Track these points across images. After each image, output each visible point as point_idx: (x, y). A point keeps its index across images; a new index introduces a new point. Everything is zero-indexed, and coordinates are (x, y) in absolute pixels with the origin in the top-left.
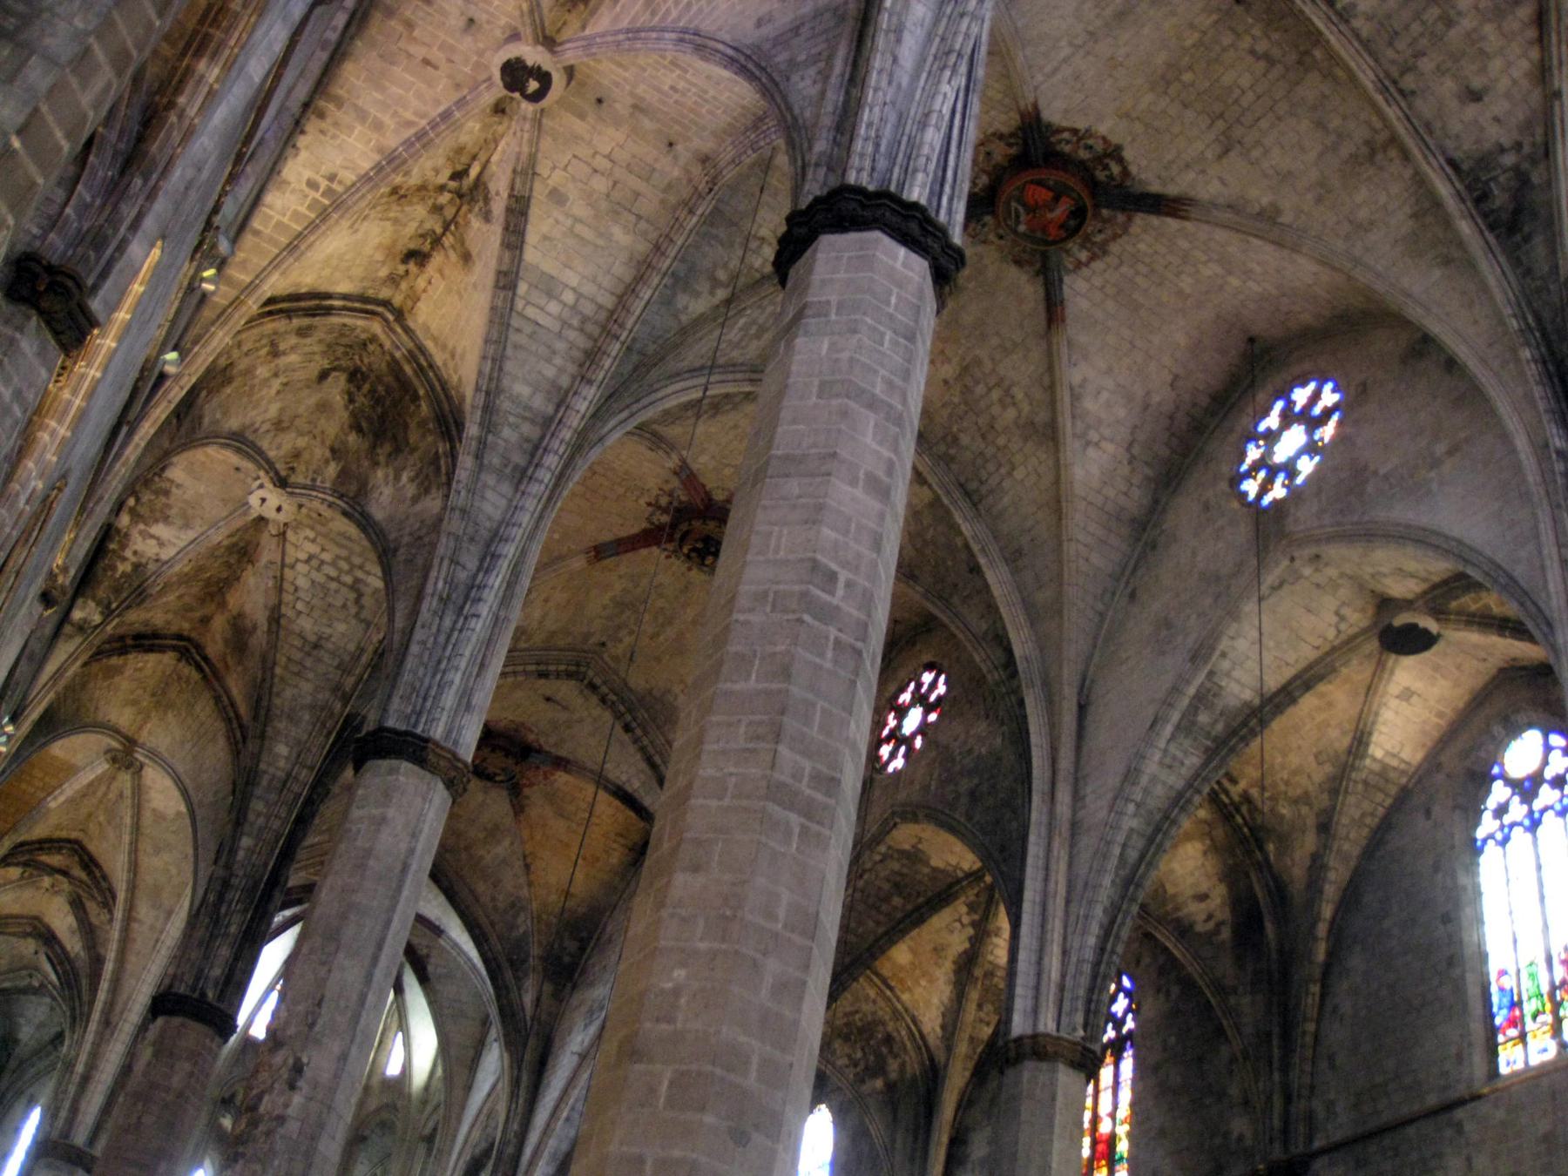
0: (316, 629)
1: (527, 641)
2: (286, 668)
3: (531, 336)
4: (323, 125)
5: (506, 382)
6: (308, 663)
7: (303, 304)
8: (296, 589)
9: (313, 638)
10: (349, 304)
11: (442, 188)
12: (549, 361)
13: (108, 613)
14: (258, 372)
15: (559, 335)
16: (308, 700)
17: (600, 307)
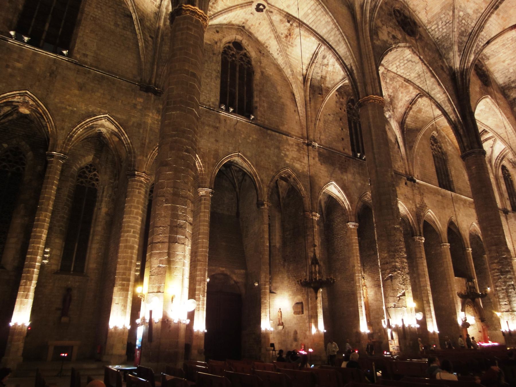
0: (415, 73)
1: (483, 9)
2: (421, 84)
3: (315, 23)
4: (269, 47)
5: (321, 34)
6: (422, 79)
7: (313, 58)
8: (403, 73)
9: (417, 75)
10: (319, 48)
11: (291, 25)
12: (321, 22)
13: (389, 110)
14: (329, 69)
15: (317, 17)
16: (431, 84)
17: (313, 5)
